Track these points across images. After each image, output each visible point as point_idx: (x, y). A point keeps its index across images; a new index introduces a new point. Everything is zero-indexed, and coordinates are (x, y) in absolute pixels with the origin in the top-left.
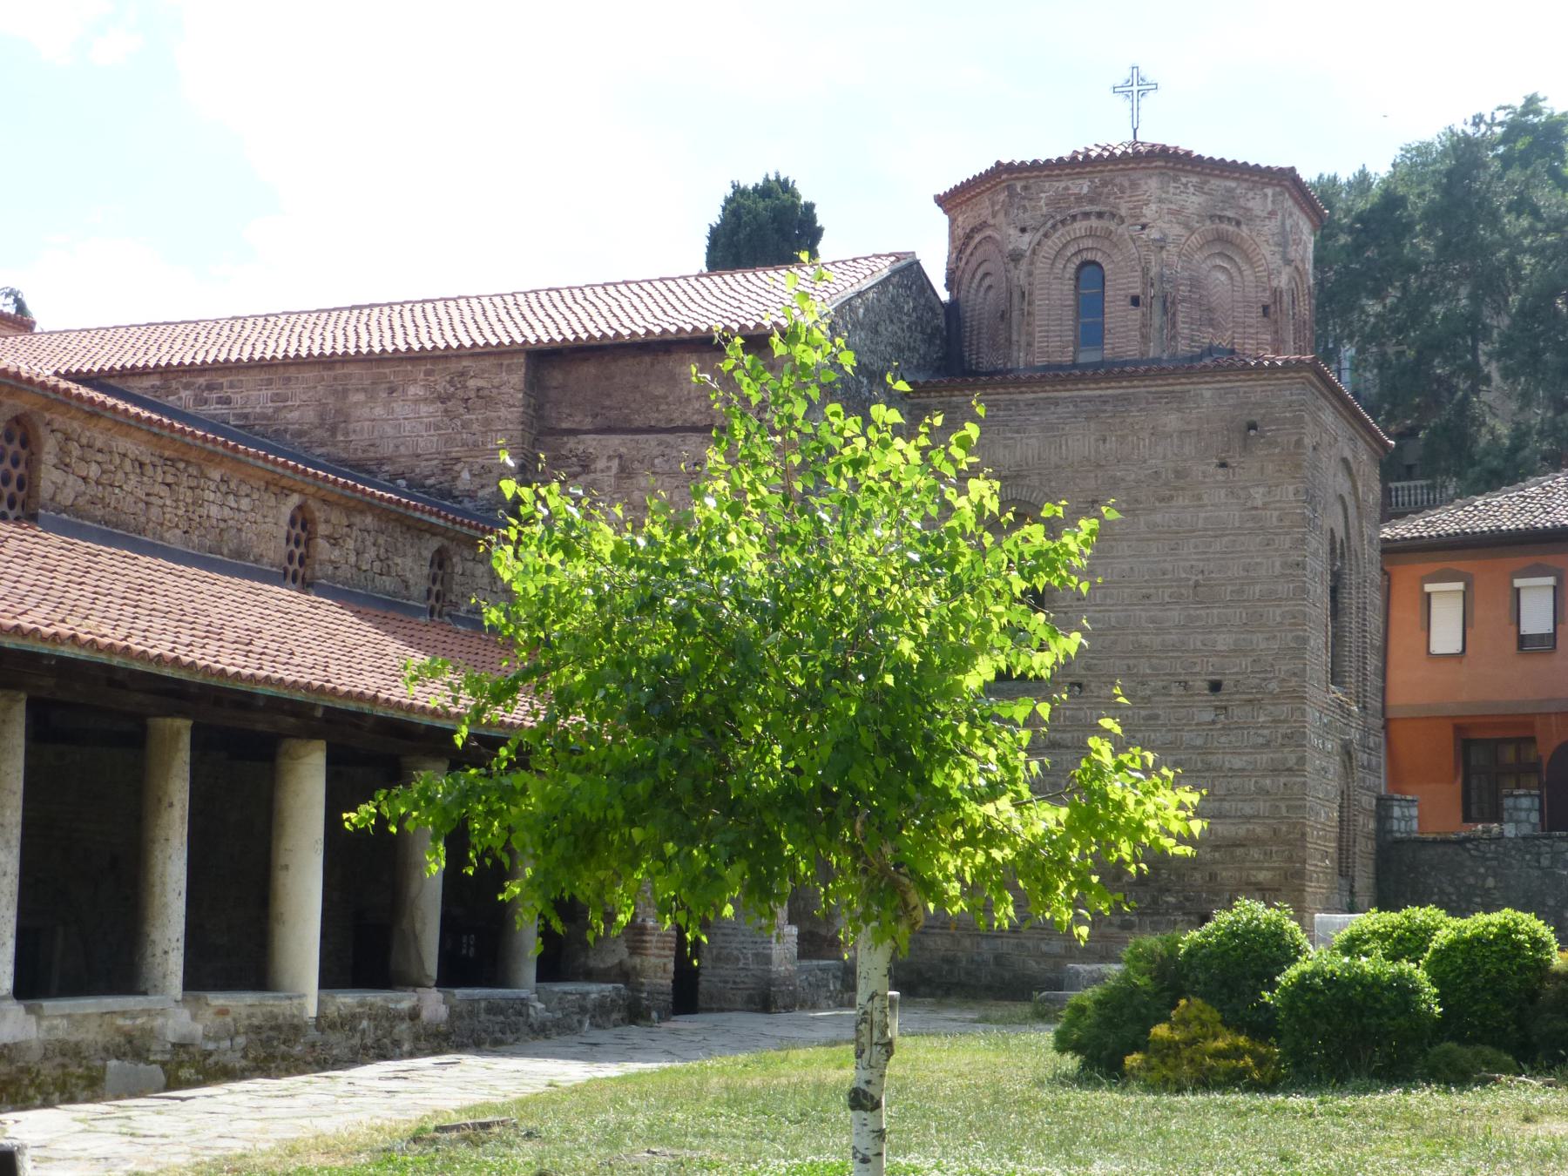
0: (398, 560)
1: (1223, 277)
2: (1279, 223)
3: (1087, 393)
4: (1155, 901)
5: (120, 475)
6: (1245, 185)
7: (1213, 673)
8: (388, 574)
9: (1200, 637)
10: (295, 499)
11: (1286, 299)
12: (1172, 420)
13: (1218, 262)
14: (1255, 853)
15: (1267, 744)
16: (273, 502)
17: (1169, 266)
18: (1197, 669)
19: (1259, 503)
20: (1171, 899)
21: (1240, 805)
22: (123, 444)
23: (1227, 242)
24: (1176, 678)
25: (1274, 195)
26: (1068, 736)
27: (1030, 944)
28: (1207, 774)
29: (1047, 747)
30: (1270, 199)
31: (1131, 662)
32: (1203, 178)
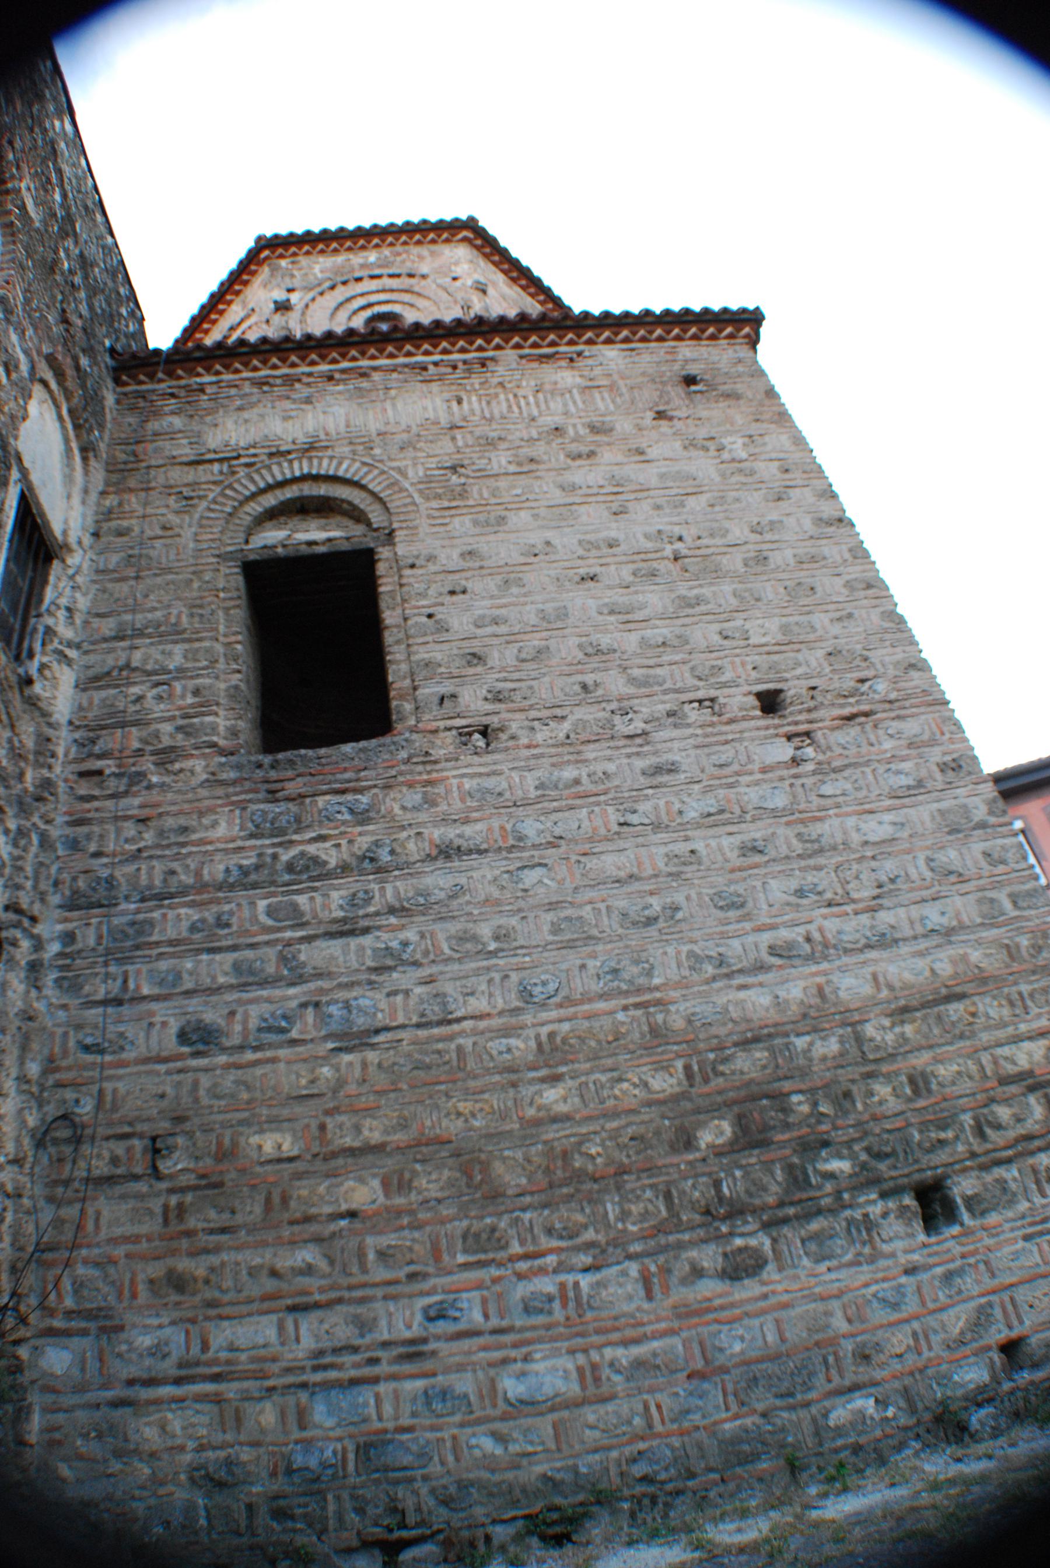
3: (420, 358)
4: (797, 1179)
7: (759, 681)
9: (716, 627)
12: (566, 377)
14: (991, 1008)
15: (920, 783)
18: (727, 676)
19: (744, 455)
20: (841, 1166)
21: (915, 912)
24: (691, 696)
26: (479, 826)
27: (464, 1384)
28: (821, 861)
29: (430, 858)
31: (589, 679)
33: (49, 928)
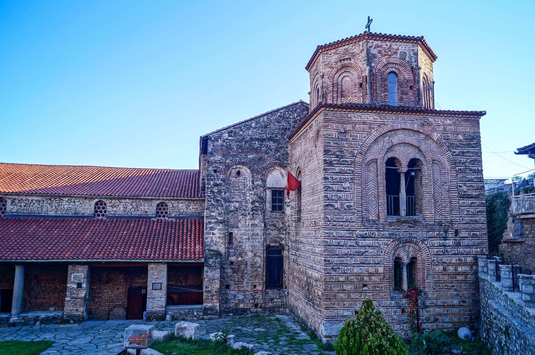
0: (142, 208)
1: (348, 79)
2: (365, 52)
5: (32, 204)
6: (351, 45)
8: (138, 210)
10: (96, 200)
11: (368, 79)
13: (345, 74)
16: (88, 201)
17: (325, 83)
22: (30, 198)
23: (347, 67)
25: (363, 44)
30: (361, 45)
32: (336, 49)
33: (290, 244)
